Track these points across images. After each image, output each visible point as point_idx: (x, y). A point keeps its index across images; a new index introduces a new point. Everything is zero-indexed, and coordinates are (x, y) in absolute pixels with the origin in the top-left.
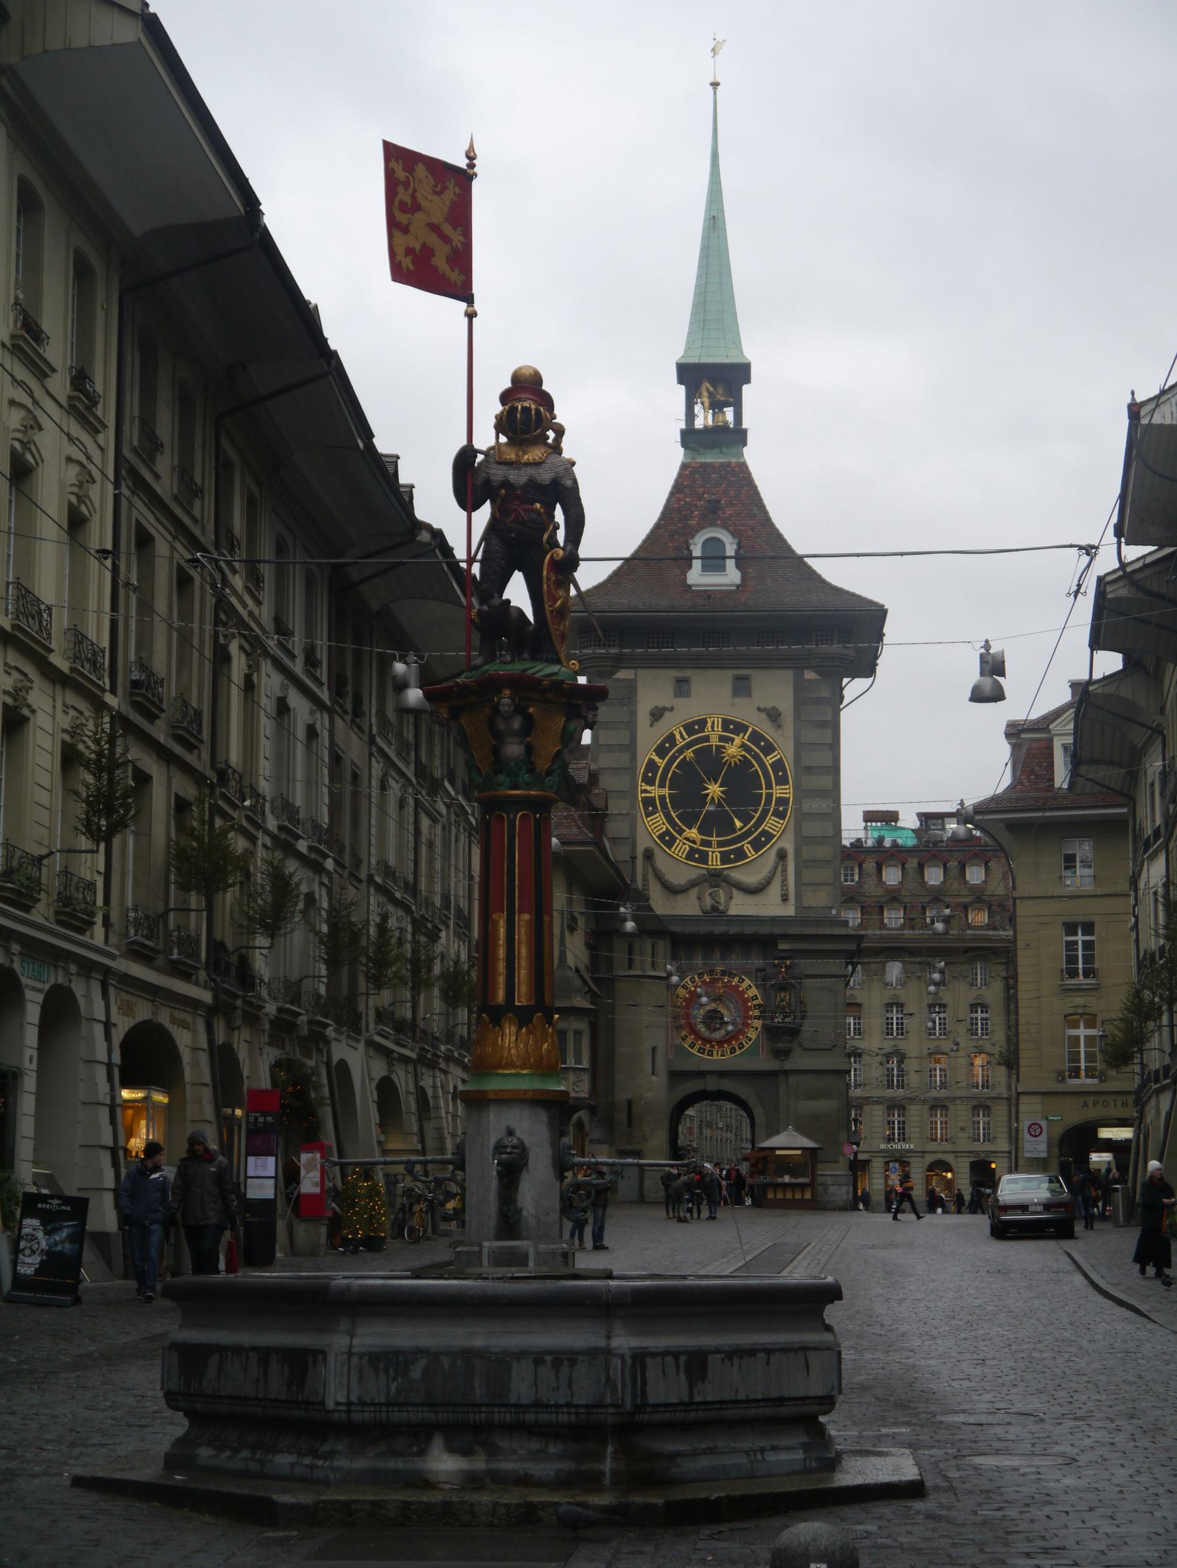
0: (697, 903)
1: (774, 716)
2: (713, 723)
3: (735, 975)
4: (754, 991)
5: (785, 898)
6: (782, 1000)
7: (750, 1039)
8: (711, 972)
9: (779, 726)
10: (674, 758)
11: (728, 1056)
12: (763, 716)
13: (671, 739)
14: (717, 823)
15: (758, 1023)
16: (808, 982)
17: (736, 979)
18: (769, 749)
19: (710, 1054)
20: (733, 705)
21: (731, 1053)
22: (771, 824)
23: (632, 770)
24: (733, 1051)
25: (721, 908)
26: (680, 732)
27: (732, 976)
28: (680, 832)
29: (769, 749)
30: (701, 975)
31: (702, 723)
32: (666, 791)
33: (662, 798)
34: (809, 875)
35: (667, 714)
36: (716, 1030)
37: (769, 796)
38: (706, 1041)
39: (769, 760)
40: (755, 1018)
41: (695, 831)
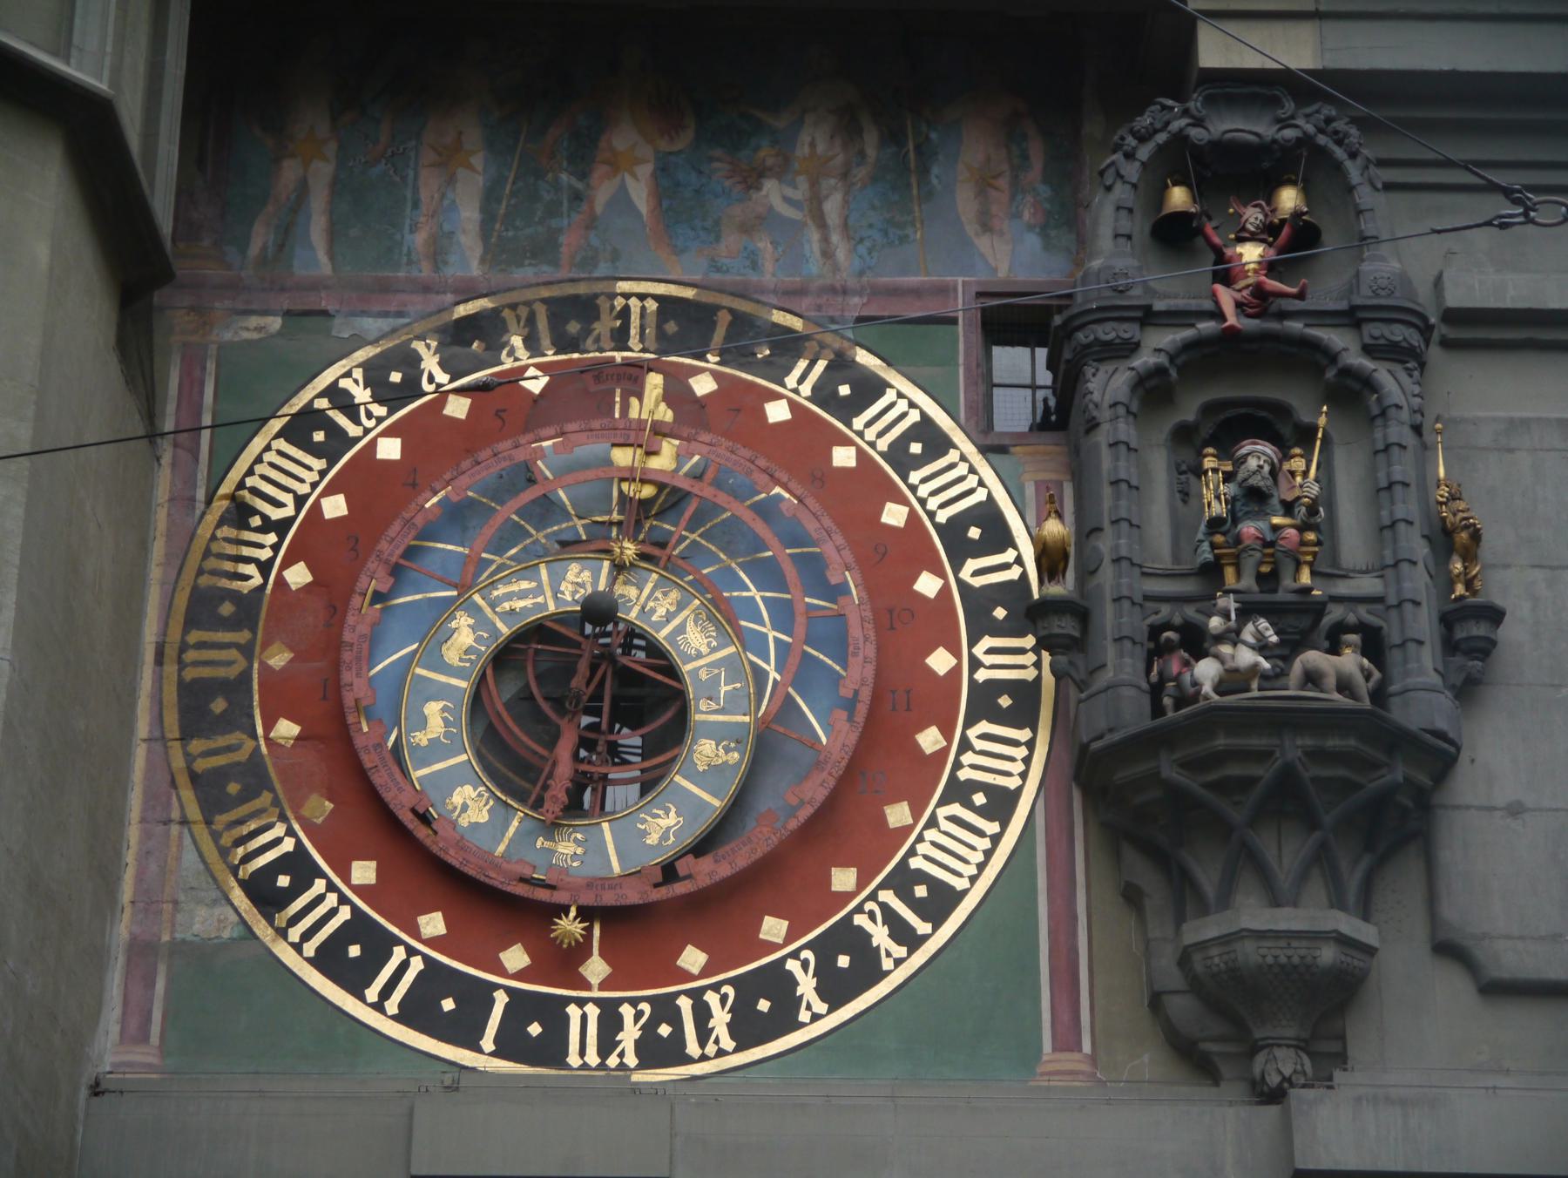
3: (788, 347)
4: (967, 478)
6: (1255, 498)
7: (940, 902)
8: (572, 317)
11: (716, 1053)
15: (1014, 759)
16: (1481, 393)
17: (802, 379)
19: (536, 1035)
21: (747, 1030)
24: (764, 1007)
27: (757, 345)
30: (465, 338)
36: (579, 803)
38: (495, 905)
40: (984, 702)
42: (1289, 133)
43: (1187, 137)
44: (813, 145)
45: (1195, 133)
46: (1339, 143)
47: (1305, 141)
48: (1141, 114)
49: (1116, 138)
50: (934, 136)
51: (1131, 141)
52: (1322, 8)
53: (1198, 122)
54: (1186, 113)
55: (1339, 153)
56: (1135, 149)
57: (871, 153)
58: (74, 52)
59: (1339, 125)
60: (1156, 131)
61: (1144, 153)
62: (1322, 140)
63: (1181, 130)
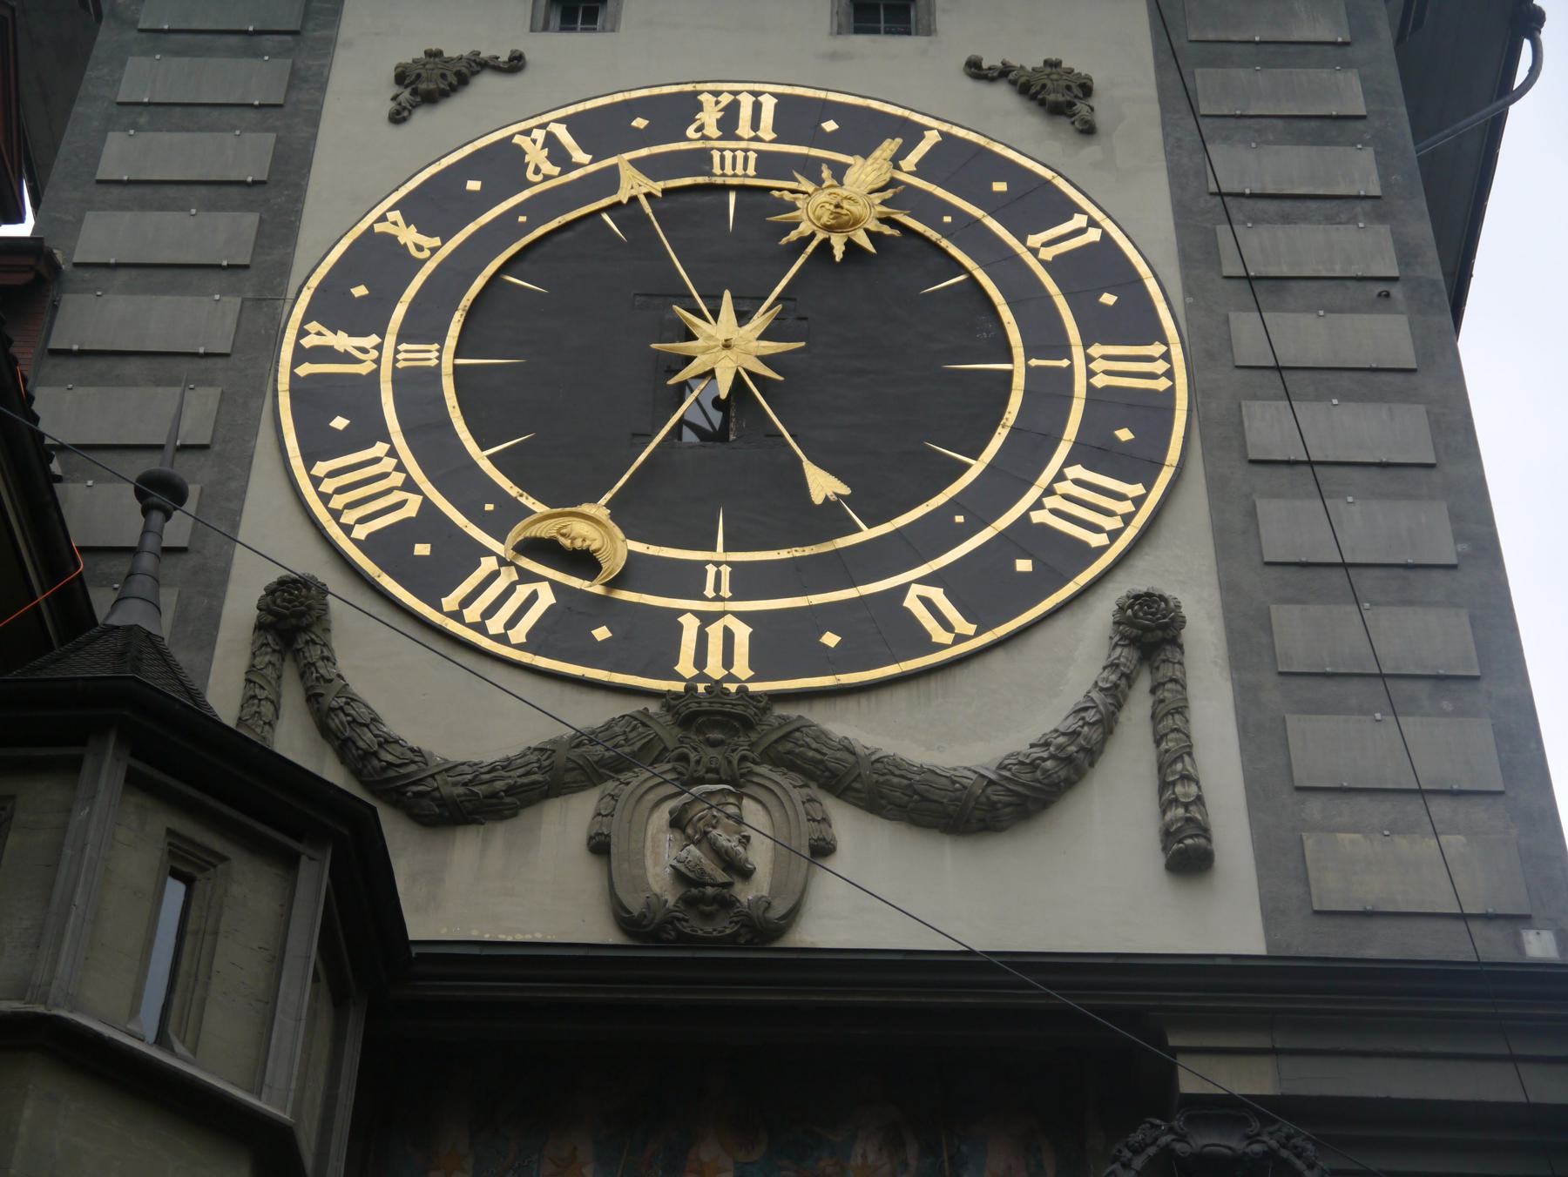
0: (585, 875)
1: (1059, 97)
2: (732, 111)
5: (1188, 857)
9: (1088, 130)
10: (505, 228)
12: (1002, 94)
13: (502, 165)
14: (725, 475)
18: (1037, 204)
20: (834, 56)
22: (1065, 495)
23: (260, 281)
25: (746, 894)
26: (551, 142)
28: (503, 518)
29: (1037, 204)
31: (675, 112)
32: (442, 356)
33: (416, 387)
34: (1331, 744)
35: (486, 83)
37: (1050, 392)
39: (1038, 250)
41: (599, 509)
42: (1257, 1148)
43: (1173, 1150)
44: (864, 1156)
45: (1179, 1146)
46: (1299, 1156)
47: (1270, 1154)
48: (1135, 1130)
49: (1114, 1151)
50: (964, 1148)
51: (1127, 1154)
52: (1278, 1046)
53: (1182, 1138)
54: (1171, 1130)
55: (1299, 1164)
56: (1130, 1160)
57: (913, 1162)
58: (265, 1090)
59: (1298, 1141)
60: (1147, 1145)
61: (1138, 1163)
62: (1284, 1153)
63: (1168, 1145)
